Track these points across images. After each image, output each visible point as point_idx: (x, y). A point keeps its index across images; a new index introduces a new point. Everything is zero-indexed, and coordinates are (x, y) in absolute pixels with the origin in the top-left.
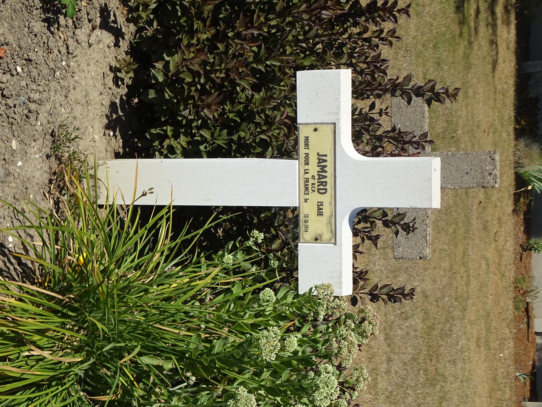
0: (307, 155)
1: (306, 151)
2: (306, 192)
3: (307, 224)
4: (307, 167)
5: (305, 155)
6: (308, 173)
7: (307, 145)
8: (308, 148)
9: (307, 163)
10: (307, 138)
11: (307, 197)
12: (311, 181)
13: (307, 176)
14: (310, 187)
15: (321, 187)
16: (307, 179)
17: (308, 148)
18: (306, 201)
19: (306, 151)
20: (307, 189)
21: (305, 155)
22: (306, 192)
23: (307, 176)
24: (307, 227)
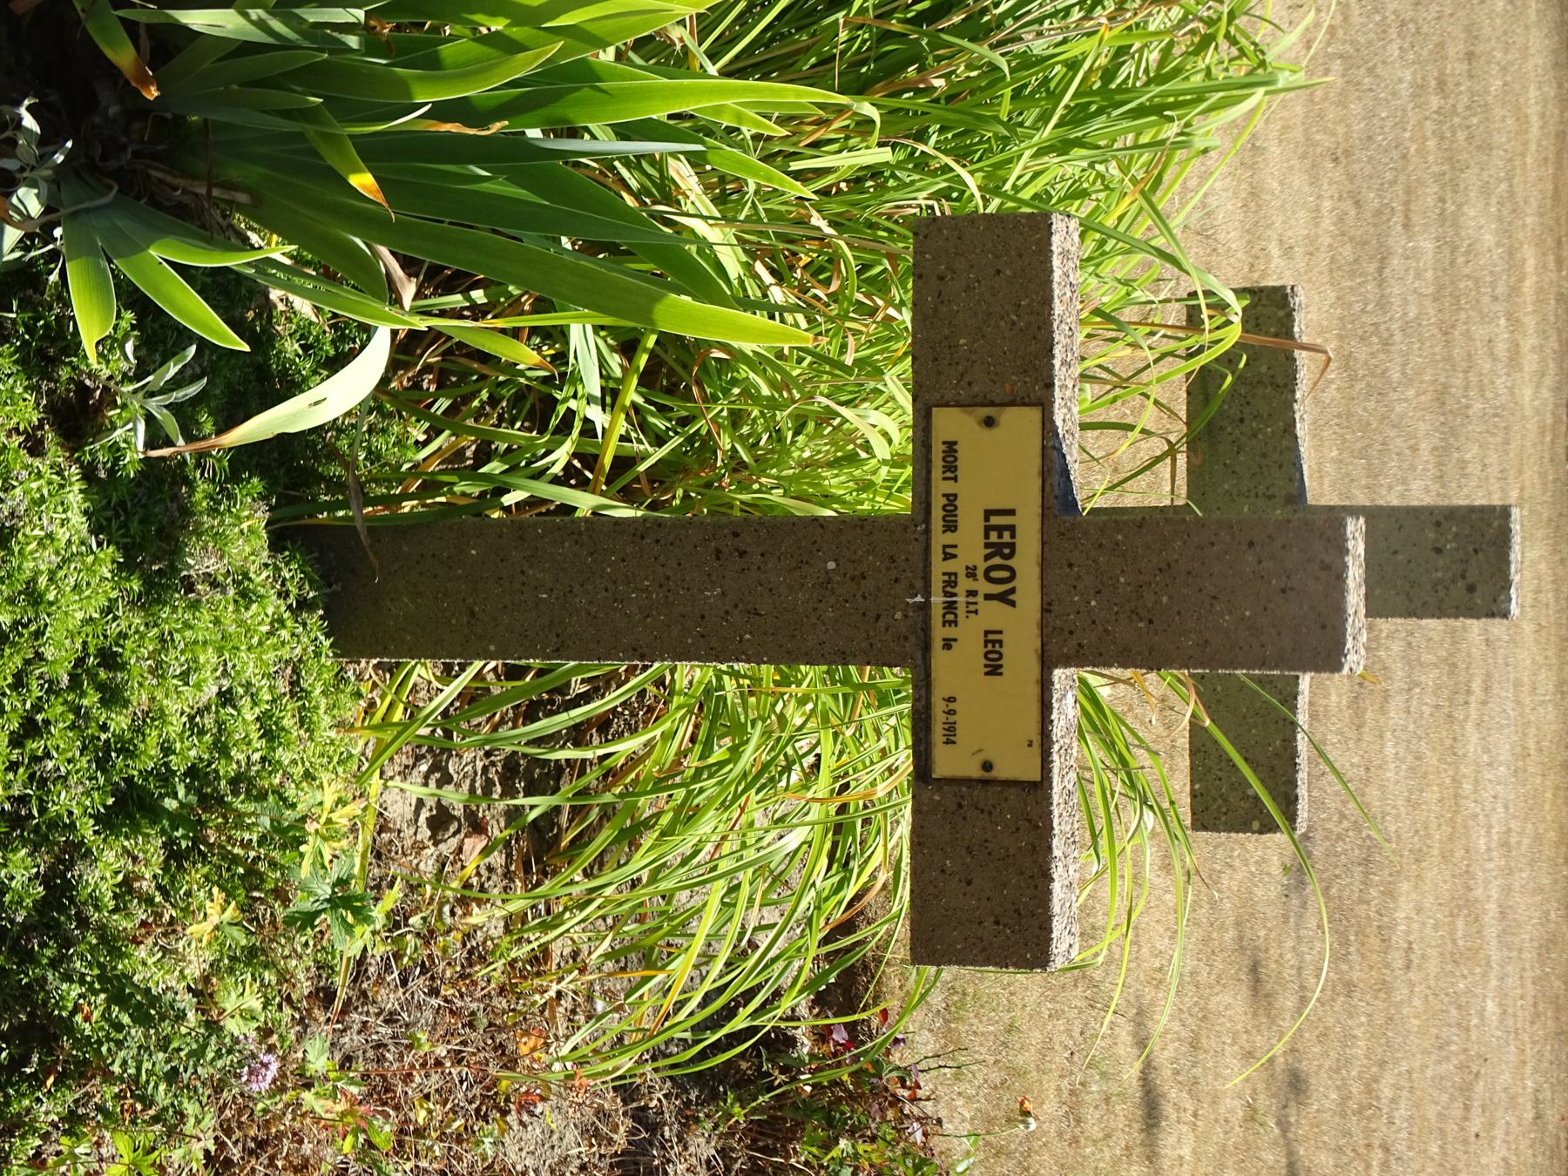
0: (951, 498)
1: (950, 487)
2: (950, 617)
3: (952, 719)
4: (949, 538)
5: (945, 501)
6: (955, 556)
7: (951, 468)
8: (955, 479)
9: (951, 526)
10: (951, 447)
11: (950, 632)
12: (964, 584)
13: (951, 566)
14: (961, 599)
15: (997, 560)
16: (950, 574)
17: (955, 479)
18: (948, 644)
19: (950, 487)
20: (950, 607)
21: (945, 501)
22: (950, 617)
23: (951, 566)
24: (951, 729)
